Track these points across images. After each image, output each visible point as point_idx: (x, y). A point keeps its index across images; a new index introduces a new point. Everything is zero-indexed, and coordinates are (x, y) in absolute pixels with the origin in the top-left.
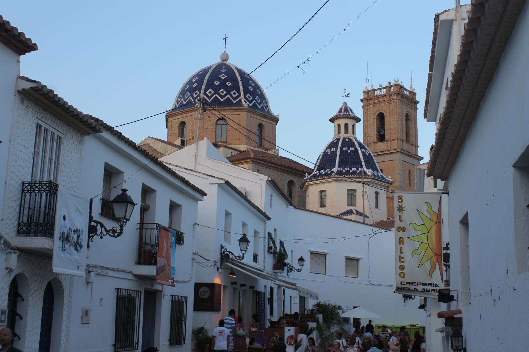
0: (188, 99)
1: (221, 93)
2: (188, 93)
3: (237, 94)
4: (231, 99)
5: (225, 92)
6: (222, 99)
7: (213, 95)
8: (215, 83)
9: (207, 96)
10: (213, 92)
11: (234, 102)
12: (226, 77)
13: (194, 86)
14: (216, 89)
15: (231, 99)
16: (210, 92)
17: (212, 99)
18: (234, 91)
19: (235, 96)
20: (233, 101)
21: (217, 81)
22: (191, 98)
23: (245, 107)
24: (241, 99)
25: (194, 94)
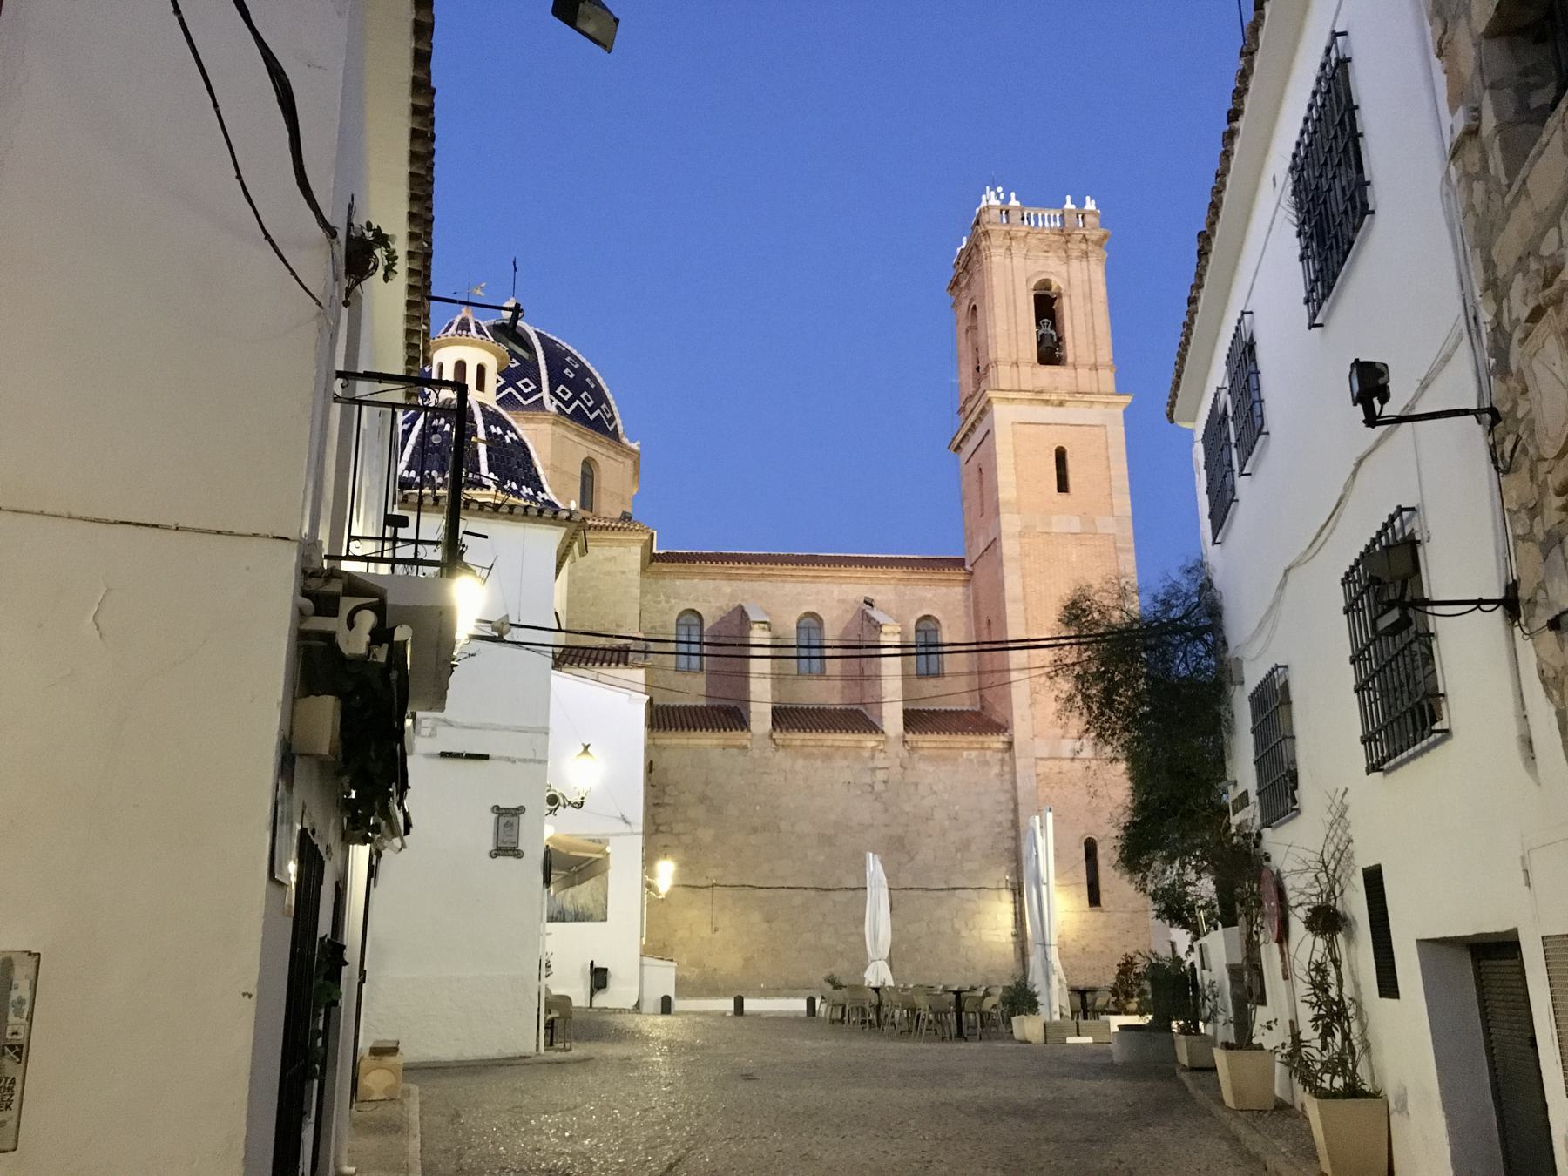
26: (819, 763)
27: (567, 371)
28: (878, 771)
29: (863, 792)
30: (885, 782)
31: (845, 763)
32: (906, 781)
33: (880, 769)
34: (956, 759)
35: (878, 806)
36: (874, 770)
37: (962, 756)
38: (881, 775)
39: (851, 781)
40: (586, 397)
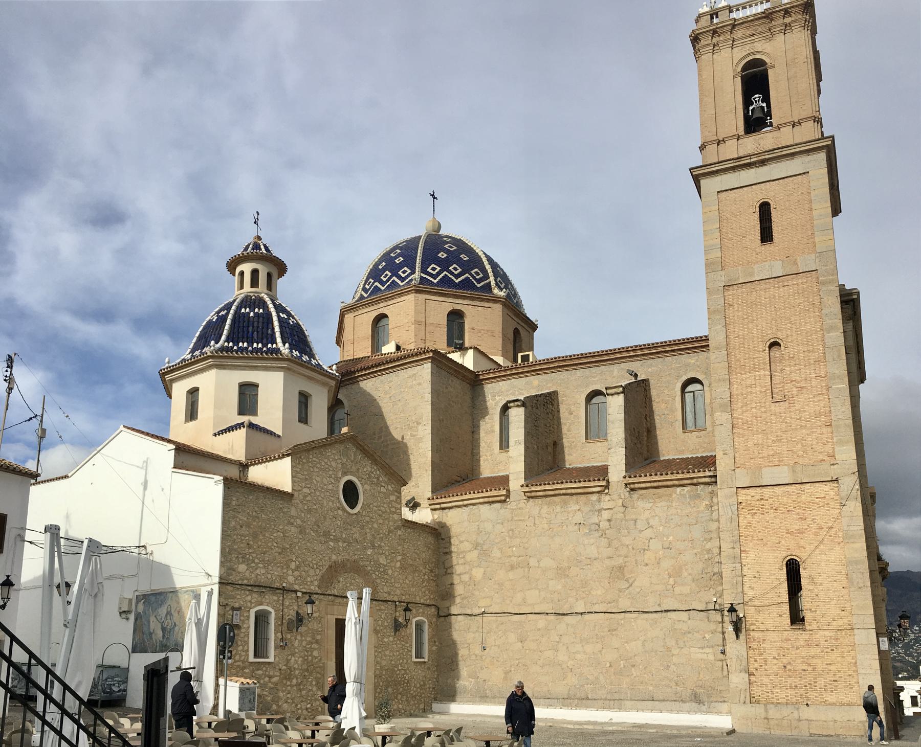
1: (454, 271)
5: (460, 270)
6: (457, 279)
8: (440, 255)
10: (439, 269)
12: (455, 248)
14: (444, 265)
16: (434, 269)
21: (442, 253)
23: (493, 294)
26: (558, 509)
28: (603, 511)
29: (590, 530)
30: (609, 520)
31: (577, 507)
32: (627, 518)
33: (605, 510)
34: (671, 495)
35: (604, 542)
36: (600, 511)
37: (676, 493)
38: (606, 515)
39: (582, 522)
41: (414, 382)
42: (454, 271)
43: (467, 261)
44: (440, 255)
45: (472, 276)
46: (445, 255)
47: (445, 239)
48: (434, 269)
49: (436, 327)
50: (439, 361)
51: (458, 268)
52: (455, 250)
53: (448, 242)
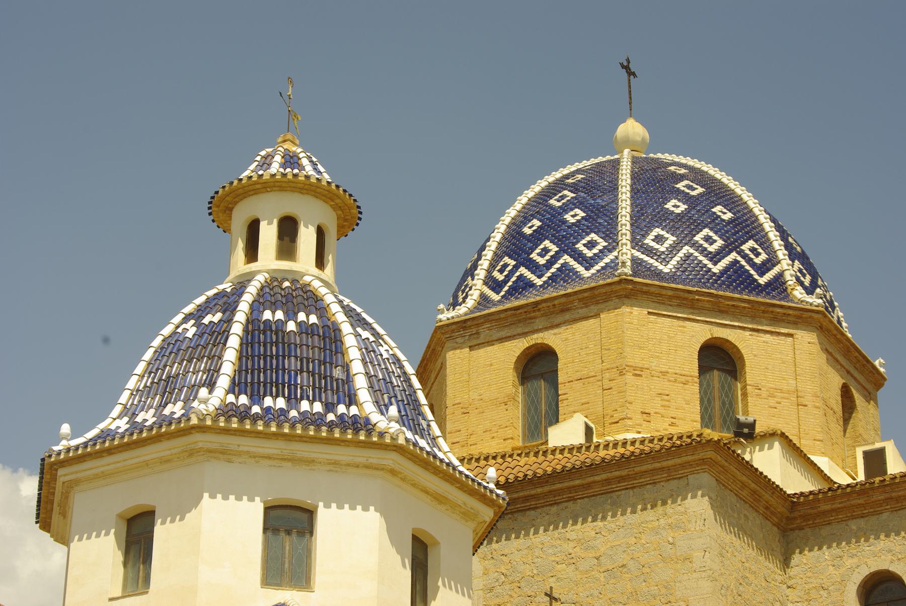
0: (557, 266)
1: (706, 245)
2: (547, 243)
3: (764, 256)
4: (748, 267)
5: (720, 243)
6: (715, 264)
7: (674, 249)
8: (669, 206)
9: (649, 251)
10: (671, 239)
11: (762, 280)
13: (572, 220)
15: (748, 267)
16: (659, 239)
17: (674, 262)
18: (751, 243)
19: (758, 261)
20: (756, 277)
22: (566, 258)
24: (781, 275)
25: (580, 246)
27: (569, 218)
40: (800, 271)
41: (662, 521)
42: (706, 245)
43: (730, 221)
44: (669, 206)
45: (750, 261)
46: (683, 207)
47: (672, 168)
48: (659, 239)
49: (675, 381)
50: (723, 467)
51: (715, 237)
52: (701, 195)
53: (682, 178)
